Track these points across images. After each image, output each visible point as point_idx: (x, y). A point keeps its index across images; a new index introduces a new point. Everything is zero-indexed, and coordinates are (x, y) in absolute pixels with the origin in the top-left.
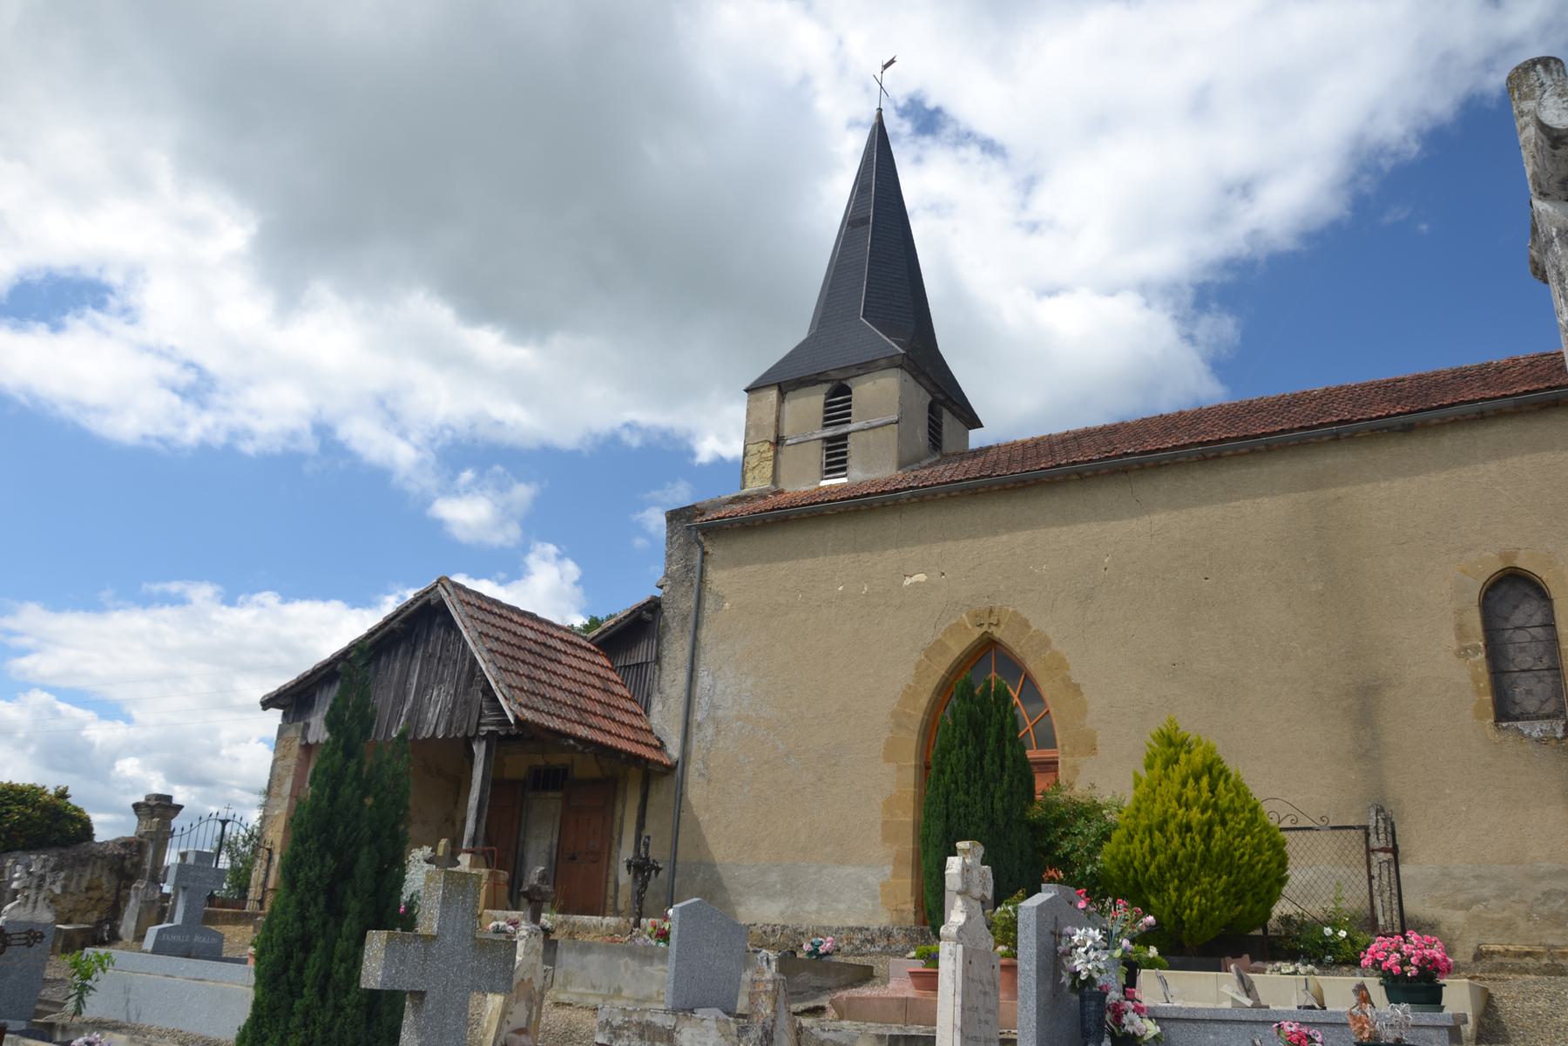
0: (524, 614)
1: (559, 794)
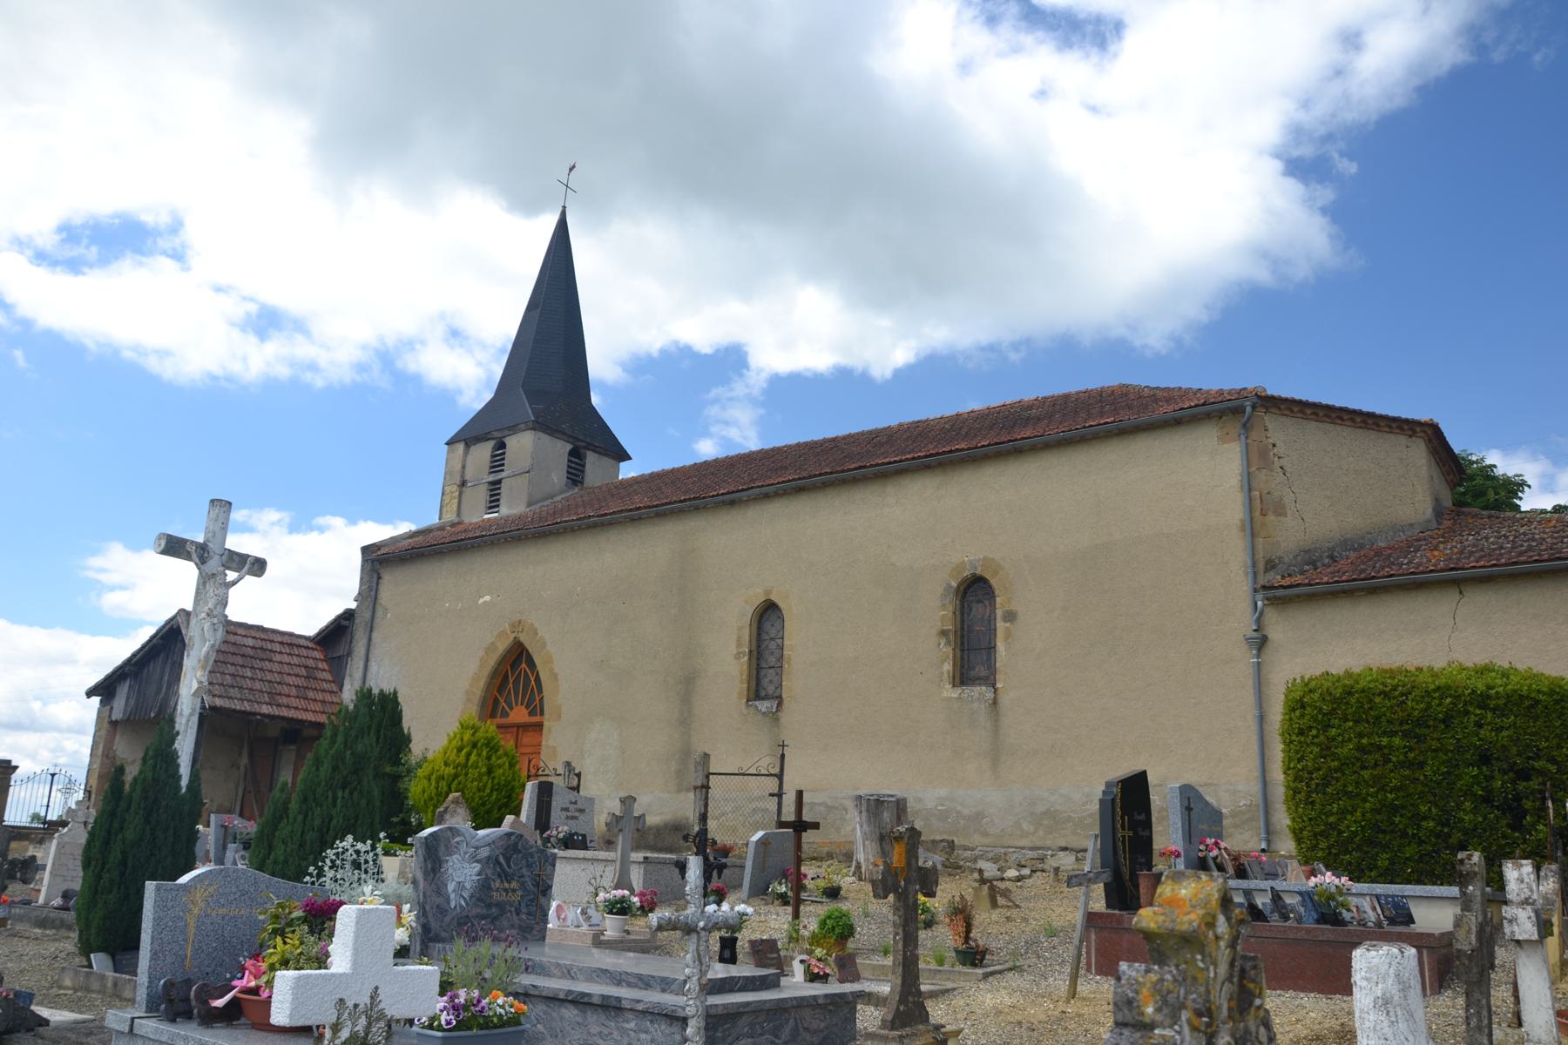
0: (252, 627)
1: (293, 747)
